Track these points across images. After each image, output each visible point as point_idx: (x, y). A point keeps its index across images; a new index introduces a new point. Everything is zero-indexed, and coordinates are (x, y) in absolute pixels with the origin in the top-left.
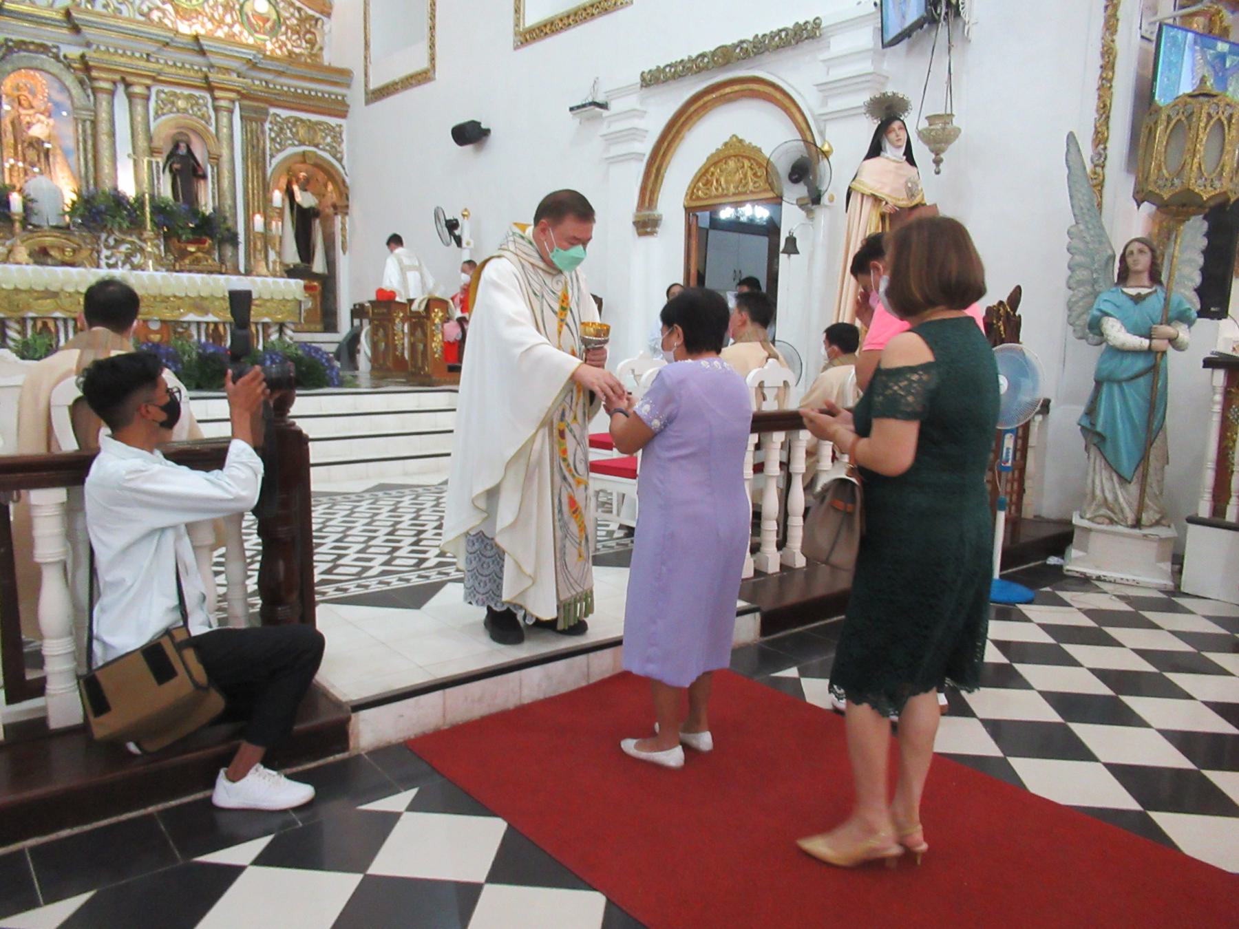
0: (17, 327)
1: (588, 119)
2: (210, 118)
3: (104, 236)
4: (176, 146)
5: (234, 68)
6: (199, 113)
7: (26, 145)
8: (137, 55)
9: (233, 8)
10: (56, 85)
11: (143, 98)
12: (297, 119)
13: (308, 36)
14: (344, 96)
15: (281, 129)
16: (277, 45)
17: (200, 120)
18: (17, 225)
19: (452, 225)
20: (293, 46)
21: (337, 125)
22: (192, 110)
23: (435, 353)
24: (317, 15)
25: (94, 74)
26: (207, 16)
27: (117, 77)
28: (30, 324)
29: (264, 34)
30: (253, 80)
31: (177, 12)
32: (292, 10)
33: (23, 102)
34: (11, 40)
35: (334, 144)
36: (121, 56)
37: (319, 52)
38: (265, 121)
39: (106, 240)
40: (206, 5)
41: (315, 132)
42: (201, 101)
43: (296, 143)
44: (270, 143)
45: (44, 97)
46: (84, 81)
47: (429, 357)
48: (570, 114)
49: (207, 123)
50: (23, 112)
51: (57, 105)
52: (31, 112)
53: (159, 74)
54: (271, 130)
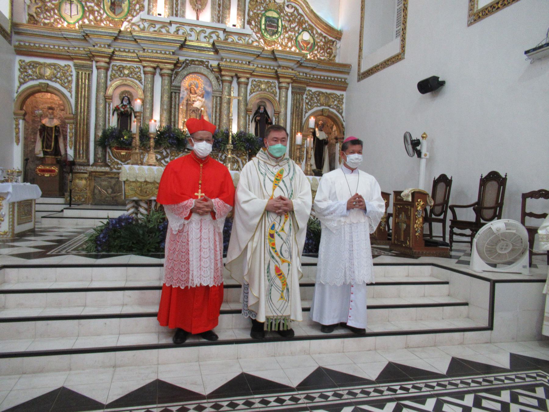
0: (145, 206)
1: (539, 59)
2: (276, 93)
3: (220, 154)
4: (259, 108)
5: (290, 66)
6: (271, 91)
7: (191, 111)
8: (244, 62)
9: (292, 39)
10: (208, 83)
11: (245, 84)
12: (320, 92)
13: (328, 51)
14: (345, 79)
15: (312, 98)
16: (312, 56)
17: (271, 94)
18: (152, 141)
19: (416, 144)
20: (320, 56)
21: (341, 95)
22: (268, 88)
23: (417, 232)
24: (334, 39)
25: (223, 73)
26: (279, 44)
27: (234, 74)
28: (153, 204)
29: (307, 50)
30: (299, 72)
31: (265, 43)
32: (321, 38)
33: (192, 91)
34: (188, 60)
35: (338, 105)
36: (237, 63)
37: (333, 58)
38: (304, 93)
39: (221, 157)
40: (279, 39)
41: (329, 99)
42: (273, 85)
43: (319, 105)
44: (306, 106)
45: (202, 88)
46: (219, 77)
47: (411, 235)
48: (525, 57)
49: (275, 95)
50: (191, 95)
51: (207, 93)
52: (195, 96)
53: (254, 71)
54: (306, 98)
